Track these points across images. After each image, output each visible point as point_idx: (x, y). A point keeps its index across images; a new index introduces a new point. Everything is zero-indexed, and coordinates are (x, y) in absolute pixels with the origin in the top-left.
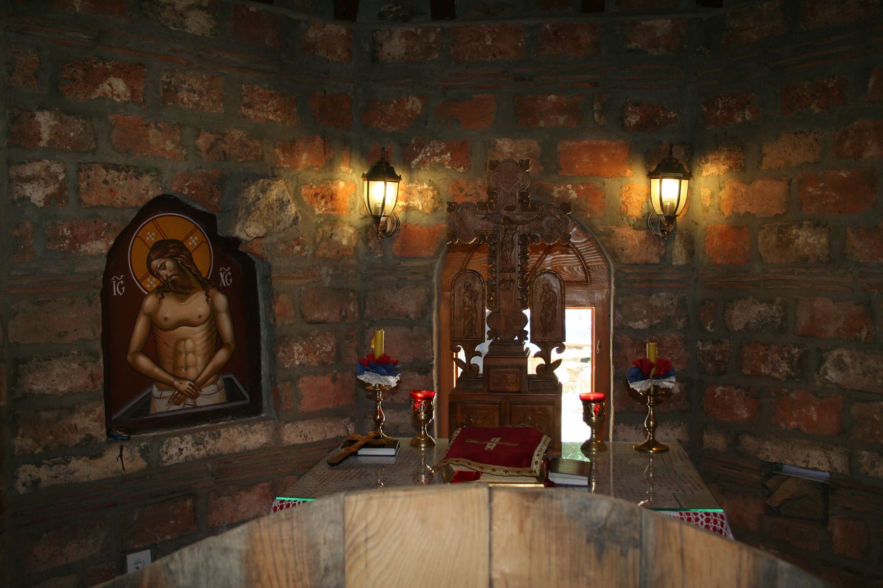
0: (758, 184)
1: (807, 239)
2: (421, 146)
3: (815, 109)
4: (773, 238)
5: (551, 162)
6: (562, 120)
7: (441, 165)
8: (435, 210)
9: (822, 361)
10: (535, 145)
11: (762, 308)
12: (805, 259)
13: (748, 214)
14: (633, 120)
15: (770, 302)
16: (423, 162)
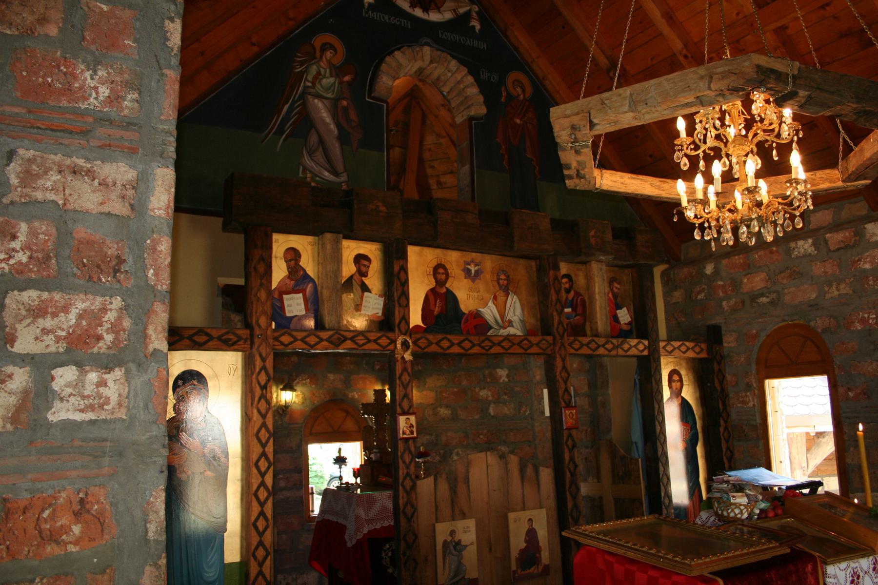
0: (425, 392)
1: (444, 412)
2: (297, 376)
3: (444, 367)
4: (431, 412)
5: (348, 383)
6: (352, 367)
7: (306, 384)
8: (303, 403)
9: (451, 454)
10: (342, 377)
11: (428, 437)
12: (443, 419)
13: (421, 403)
14: (377, 367)
15: (431, 435)
16: (298, 383)
